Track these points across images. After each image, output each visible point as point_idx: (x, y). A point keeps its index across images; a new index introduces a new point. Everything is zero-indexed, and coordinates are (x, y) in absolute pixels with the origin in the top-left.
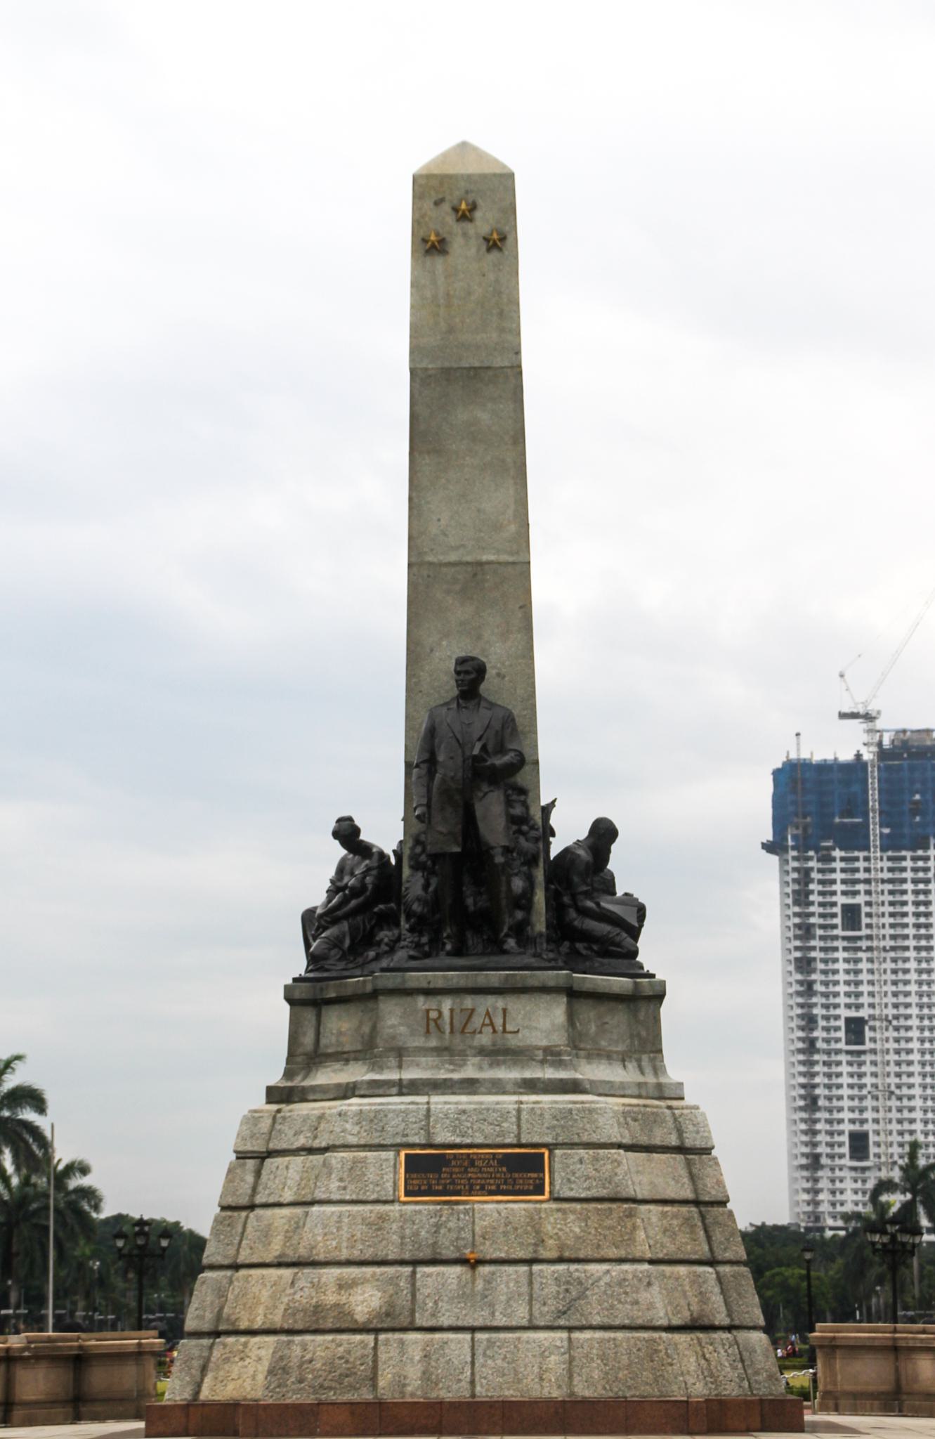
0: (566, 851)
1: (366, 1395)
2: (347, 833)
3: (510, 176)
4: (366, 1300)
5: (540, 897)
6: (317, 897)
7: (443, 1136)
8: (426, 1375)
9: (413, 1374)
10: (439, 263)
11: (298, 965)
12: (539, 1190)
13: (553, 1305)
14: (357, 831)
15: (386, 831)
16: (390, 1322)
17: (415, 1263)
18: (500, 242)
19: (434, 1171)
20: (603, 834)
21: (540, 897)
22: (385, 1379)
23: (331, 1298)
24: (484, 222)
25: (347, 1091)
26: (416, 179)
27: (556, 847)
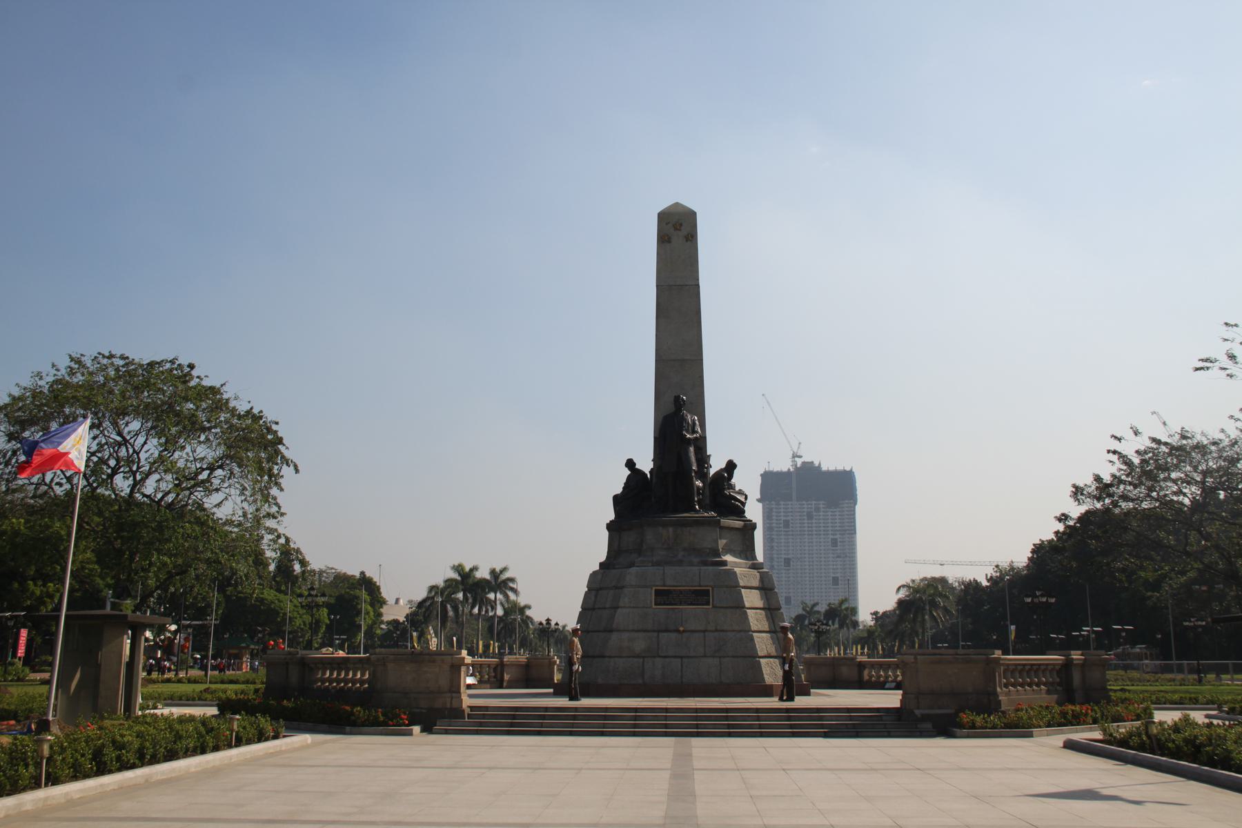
0: (717, 474)
1: (640, 681)
2: (630, 464)
3: (693, 215)
4: (640, 644)
6: (619, 490)
7: (669, 582)
11: (612, 517)
12: (708, 604)
15: (646, 464)
17: (659, 631)
18: (691, 237)
19: (664, 596)
20: (731, 466)
25: (632, 565)
26: (659, 215)
27: (712, 471)
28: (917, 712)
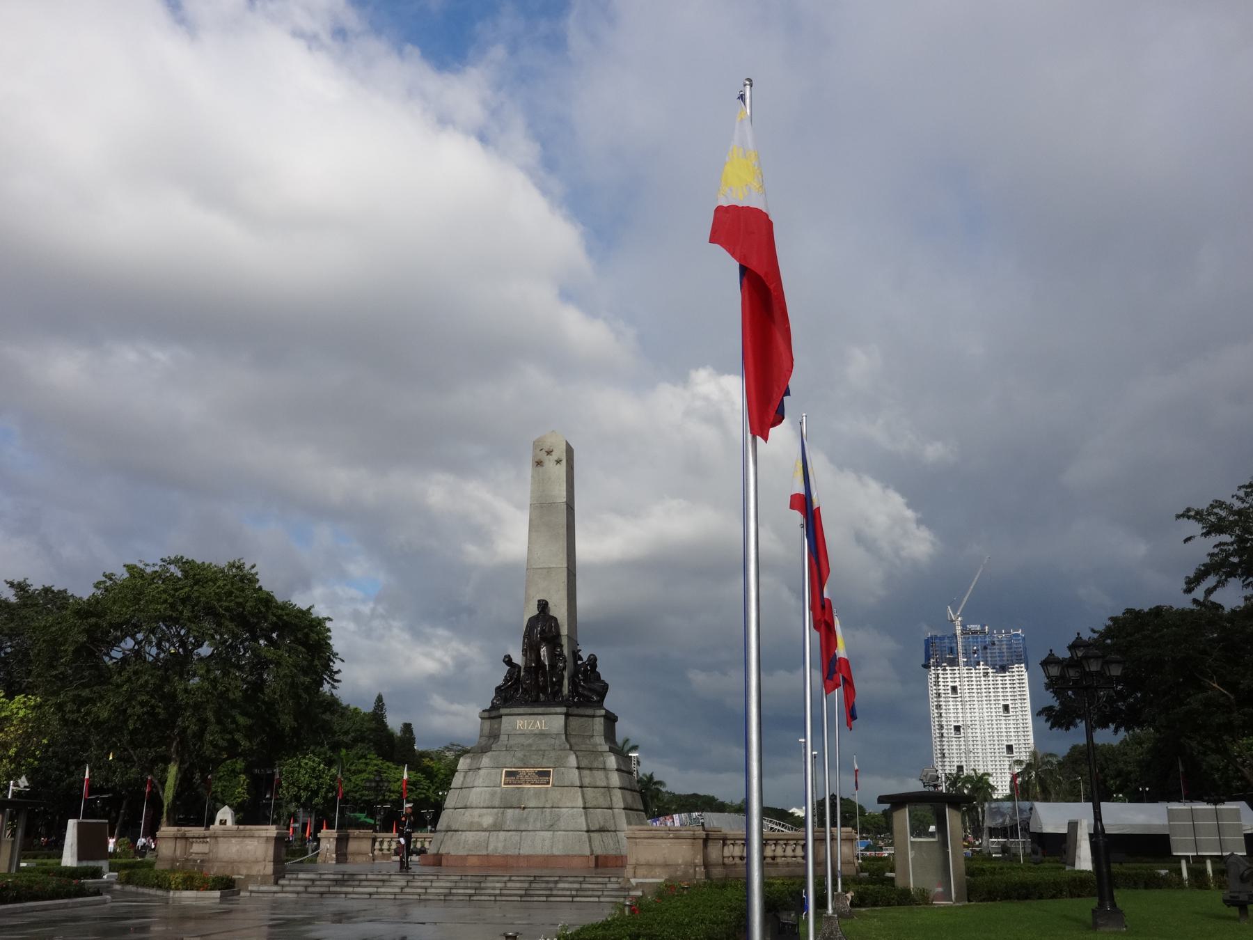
1: (484, 853)
4: (487, 821)
5: (566, 682)
8: (504, 847)
9: (500, 845)
10: (540, 469)
11: (488, 705)
13: (548, 823)
14: (510, 660)
15: (518, 659)
16: (496, 828)
20: (593, 661)
21: (566, 682)
22: (491, 847)
23: (476, 819)
24: (555, 456)
28: (633, 881)
